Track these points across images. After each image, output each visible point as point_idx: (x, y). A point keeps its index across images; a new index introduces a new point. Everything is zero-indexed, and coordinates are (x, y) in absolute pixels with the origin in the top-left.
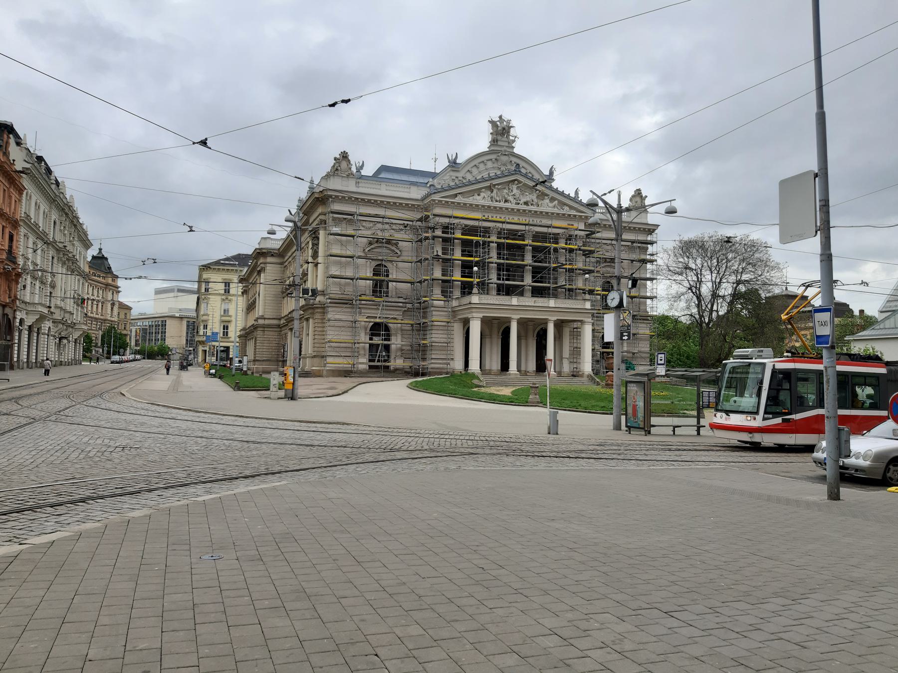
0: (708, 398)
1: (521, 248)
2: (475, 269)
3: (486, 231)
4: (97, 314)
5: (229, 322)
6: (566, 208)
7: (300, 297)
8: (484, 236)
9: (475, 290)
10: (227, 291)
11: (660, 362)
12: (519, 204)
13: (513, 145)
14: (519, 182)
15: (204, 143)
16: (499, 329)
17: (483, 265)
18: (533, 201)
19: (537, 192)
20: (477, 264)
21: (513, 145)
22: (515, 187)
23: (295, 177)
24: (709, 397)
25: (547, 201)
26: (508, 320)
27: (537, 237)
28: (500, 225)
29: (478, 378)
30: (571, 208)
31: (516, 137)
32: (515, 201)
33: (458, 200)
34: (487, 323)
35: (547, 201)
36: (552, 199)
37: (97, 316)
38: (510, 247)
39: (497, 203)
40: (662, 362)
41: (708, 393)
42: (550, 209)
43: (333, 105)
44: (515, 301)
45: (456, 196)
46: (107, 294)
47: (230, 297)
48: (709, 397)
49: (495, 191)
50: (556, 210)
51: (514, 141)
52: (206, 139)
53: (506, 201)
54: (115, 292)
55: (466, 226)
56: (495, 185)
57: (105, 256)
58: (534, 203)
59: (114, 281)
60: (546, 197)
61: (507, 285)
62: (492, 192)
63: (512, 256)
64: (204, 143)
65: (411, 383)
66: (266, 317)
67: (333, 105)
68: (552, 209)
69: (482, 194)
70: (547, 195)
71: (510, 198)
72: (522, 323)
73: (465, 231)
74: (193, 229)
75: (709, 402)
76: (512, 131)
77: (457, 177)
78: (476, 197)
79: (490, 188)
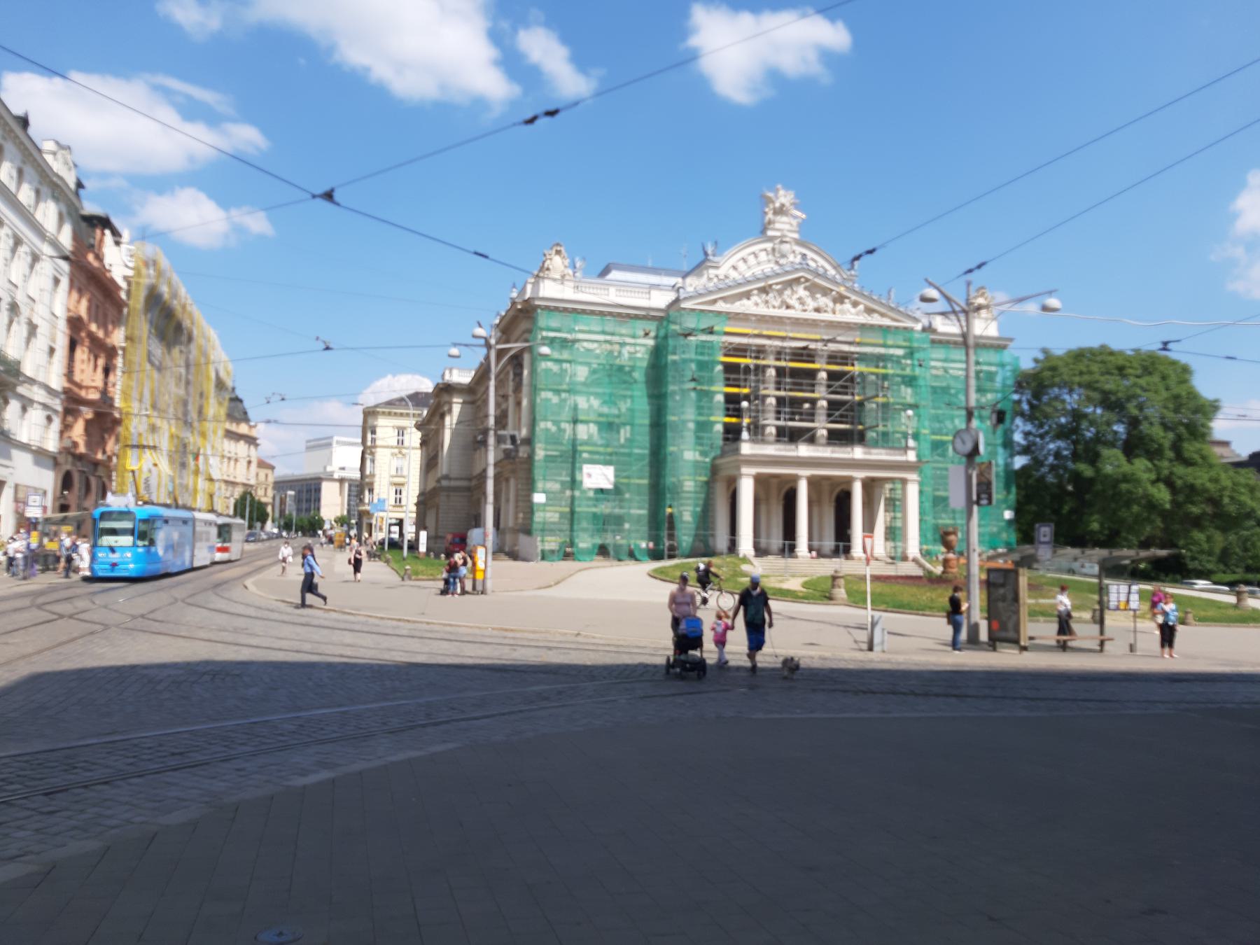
1: (812, 374)
2: (745, 404)
3: (760, 352)
6: (876, 315)
8: (757, 358)
9: (745, 435)
11: (1043, 539)
12: (805, 311)
15: (329, 196)
16: (779, 490)
17: (755, 397)
20: (747, 398)
23: (476, 253)
25: (847, 306)
26: (795, 479)
27: (833, 358)
28: (778, 343)
29: (750, 562)
30: (883, 315)
32: (800, 307)
33: (721, 306)
34: (762, 482)
35: (847, 306)
36: (855, 304)
38: (795, 373)
39: (776, 310)
40: (1047, 539)
42: (852, 317)
43: (531, 121)
44: (804, 450)
45: (714, 302)
50: (863, 319)
52: (332, 190)
55: (731, 344)
61: (791, 428)
63: (797, 387)
64: (329, 196)
65: (656, 570)
67: (531, 121)
68: (856, 317)
69: (755, 298)
70: (848, 298)
71: (793, 302)
72: (814, 483)
73: (729, 350)
74: (331, 346)
77: (717, 276)
78: (745, 301)
79: (764, 290)
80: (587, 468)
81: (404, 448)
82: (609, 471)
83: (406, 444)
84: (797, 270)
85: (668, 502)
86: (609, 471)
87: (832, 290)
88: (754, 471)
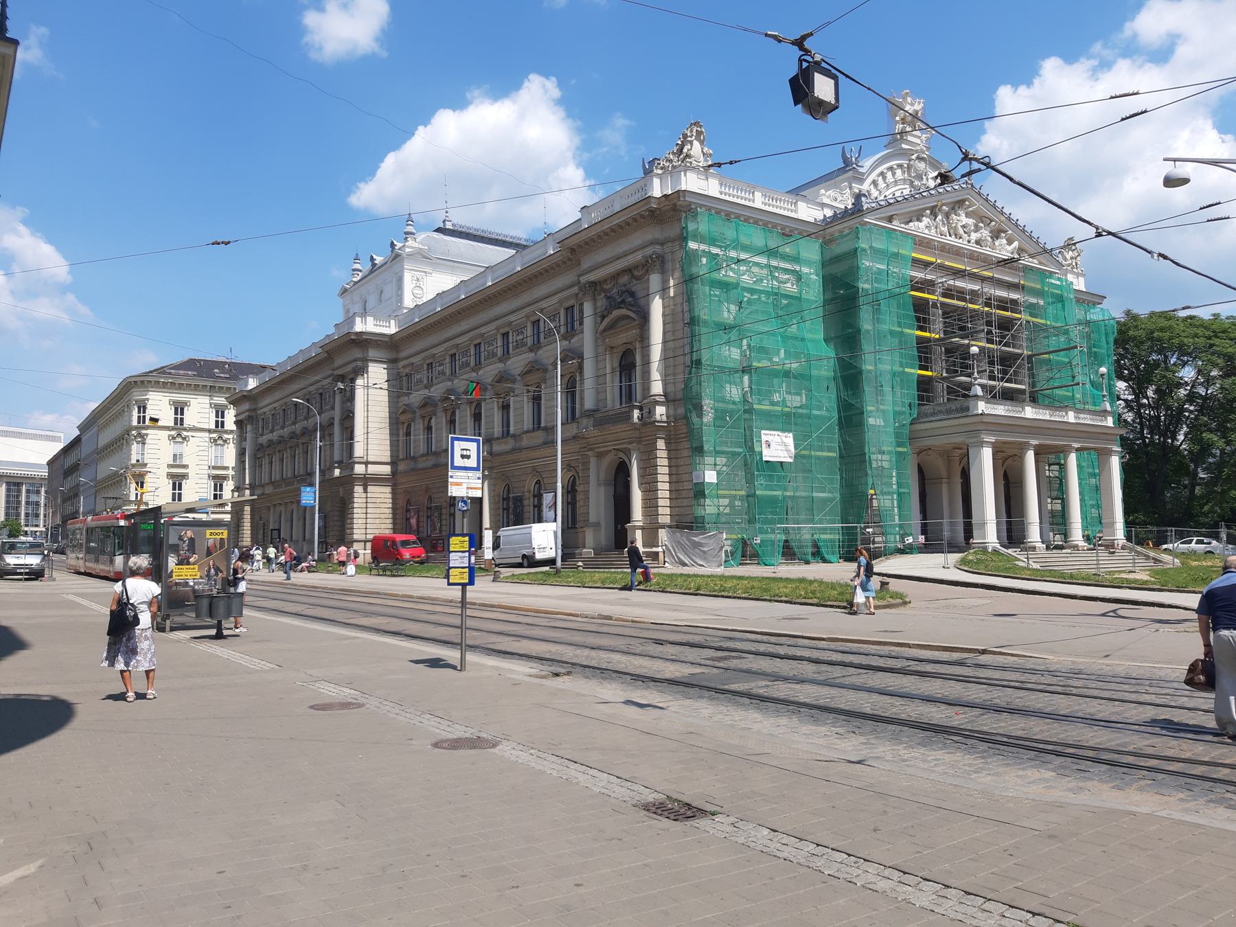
5: (185, 476)
10: (179, 422)
19: (993, 223)
47: (185, 433)
60: (1003, 235)
66: (371, 459)
69: (926, 220)
70: (1005, 232)
80: (766, 435)
81: (185, 430)
82: (789, 439)
83: (187, 423)
85: (870, 481)
86: (789, 439)
88: (992, 439)
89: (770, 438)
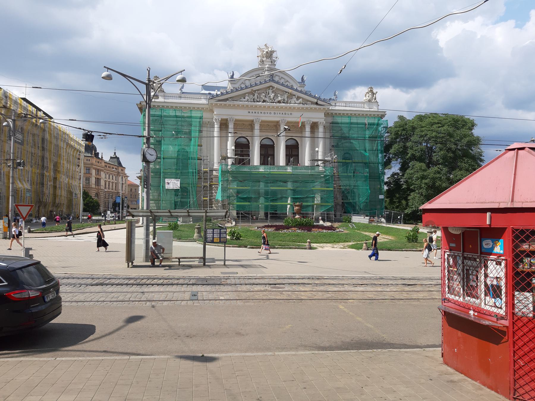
0: (212, 235)
4: (112, 189)
7: (15, 168)
13: (275, 63)
14: (273, 87)
18: (284, 100)
21: (275, 63)
22: (270, 91)
24: (213, 234)
25: (294, 99)
31: (277, 58)
35: (294, 99)
37: (112, 191)
41: (212, 230)
46: (118, 178)
48: (213, 234)
49: (256, 95)
51: (275, 61)
53: (264, 101)
54: (123, 177)
56: (255, 91)
57: (118, 157)
58: (285, 101)
59: (122, 170)
62: (254, 95)
69: (247, 98)
70: (295, 95)
75: (213, 238)
76: (274, 55)
80: (167, 180)
84: (266, 82)
87: (286, 92)
89: (169, 181)
